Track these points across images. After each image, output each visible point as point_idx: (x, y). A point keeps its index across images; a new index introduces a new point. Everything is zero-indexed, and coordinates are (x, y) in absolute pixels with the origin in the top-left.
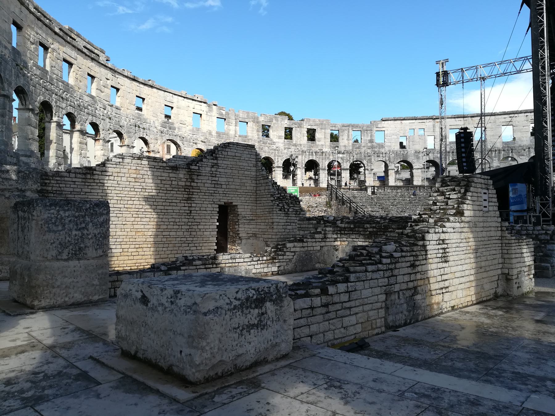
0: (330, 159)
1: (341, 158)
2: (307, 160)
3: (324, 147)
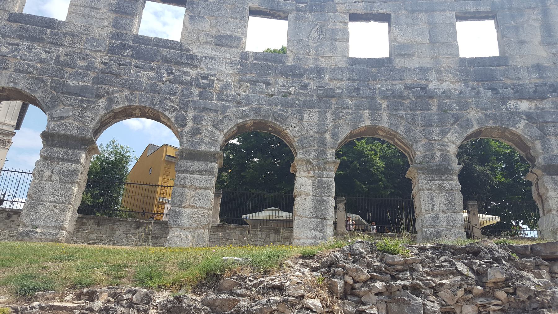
0: (469, 123)
1: (529, 117)
2: (345, 132)
3: (432, 75)
